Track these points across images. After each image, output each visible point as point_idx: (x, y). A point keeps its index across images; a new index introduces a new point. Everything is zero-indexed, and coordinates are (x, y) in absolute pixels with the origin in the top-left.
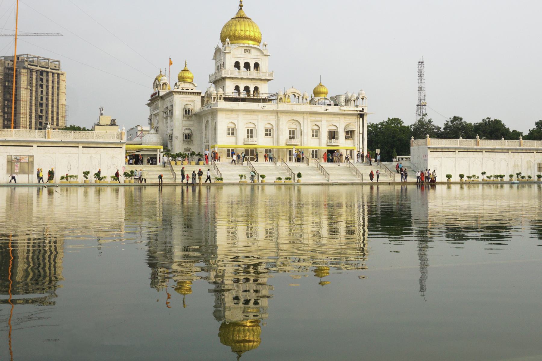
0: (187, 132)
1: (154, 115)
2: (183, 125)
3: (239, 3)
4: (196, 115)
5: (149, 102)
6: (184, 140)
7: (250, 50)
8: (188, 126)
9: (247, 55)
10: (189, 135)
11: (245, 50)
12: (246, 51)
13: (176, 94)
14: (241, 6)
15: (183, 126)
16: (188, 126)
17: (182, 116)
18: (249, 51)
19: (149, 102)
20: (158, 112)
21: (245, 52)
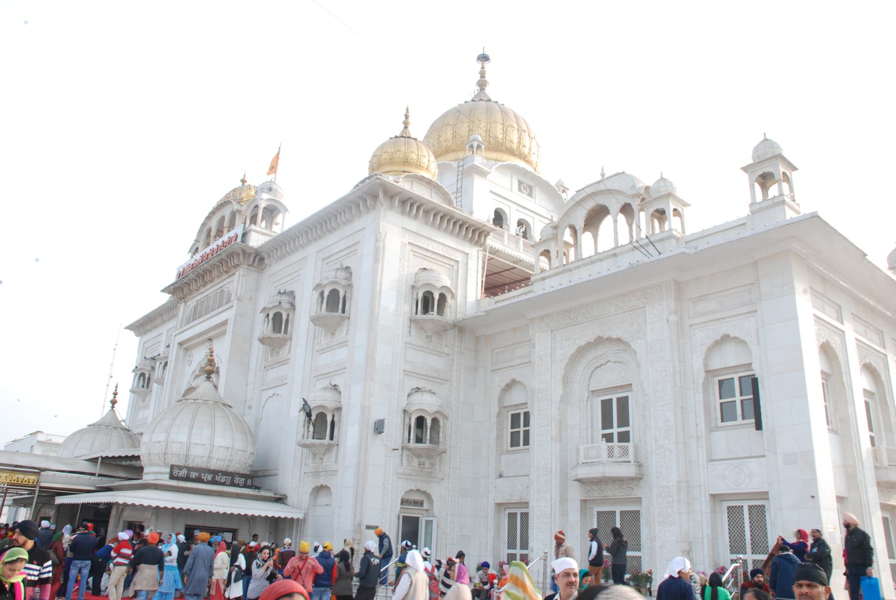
0: (427, 404)
1: (181, 344)
2: (409, 368)
3: (478, 77)
4: (460, 328)
5: (166, 297)
6: (413, 444)
7: (531, 188)
8: (428, 378)
9: (523, 199)
10: (435, 421)
11: (520, 183)
12: (522, 187)
13: (392, 208)
14: (482, 84)
15: (406, 373)
16: (428, 378)
17: (407, 321)
18: (528, 190)
19: (166, 297)
20: (225, 323)
21: (520, 190)
